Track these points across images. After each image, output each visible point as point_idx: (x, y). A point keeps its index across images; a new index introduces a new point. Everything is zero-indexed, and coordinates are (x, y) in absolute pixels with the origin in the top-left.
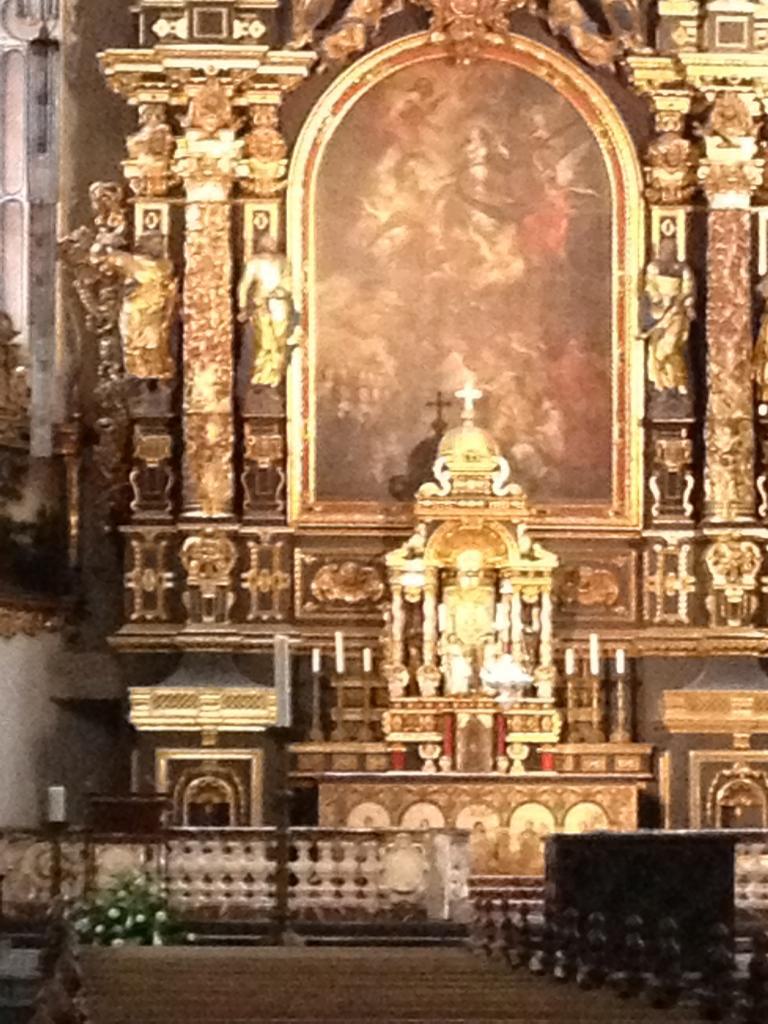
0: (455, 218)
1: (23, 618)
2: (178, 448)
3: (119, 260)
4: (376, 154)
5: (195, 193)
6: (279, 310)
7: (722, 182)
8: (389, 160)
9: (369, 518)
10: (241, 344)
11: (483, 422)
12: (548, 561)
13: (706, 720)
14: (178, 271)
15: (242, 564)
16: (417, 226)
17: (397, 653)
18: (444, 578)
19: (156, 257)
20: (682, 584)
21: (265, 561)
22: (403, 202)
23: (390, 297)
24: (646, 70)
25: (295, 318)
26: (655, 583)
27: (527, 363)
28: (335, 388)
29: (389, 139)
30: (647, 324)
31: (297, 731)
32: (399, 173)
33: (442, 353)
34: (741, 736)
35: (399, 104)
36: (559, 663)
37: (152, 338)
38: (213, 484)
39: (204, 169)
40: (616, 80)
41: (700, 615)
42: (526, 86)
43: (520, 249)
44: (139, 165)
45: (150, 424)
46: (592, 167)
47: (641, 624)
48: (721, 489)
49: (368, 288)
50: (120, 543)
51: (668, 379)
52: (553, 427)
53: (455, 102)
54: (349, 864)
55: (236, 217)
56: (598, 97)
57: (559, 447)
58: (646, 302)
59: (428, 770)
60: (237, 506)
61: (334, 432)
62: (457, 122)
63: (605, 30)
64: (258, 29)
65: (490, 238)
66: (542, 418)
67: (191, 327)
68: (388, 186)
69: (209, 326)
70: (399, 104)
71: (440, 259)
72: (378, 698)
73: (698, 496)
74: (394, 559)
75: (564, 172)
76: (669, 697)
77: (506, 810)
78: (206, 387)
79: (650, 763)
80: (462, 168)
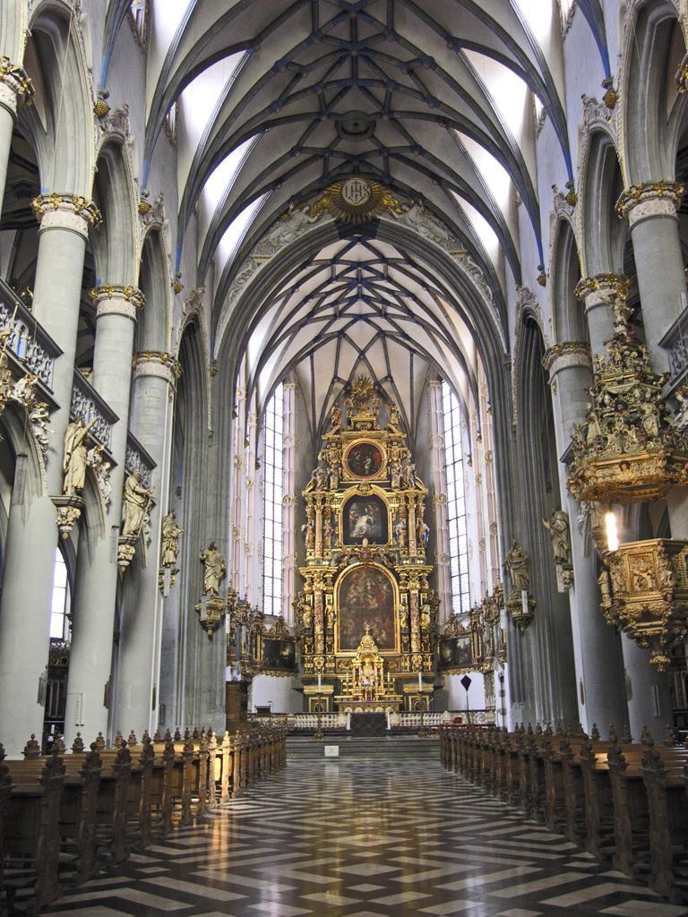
1: (286, 673)
2: (314, 640)
3: (303, 606)
4: (351, 585)
5: (316, 593)
6: (332, 614)
7: (412, 589)
8: (353, 586)
9: (352, 654)
10: (325, 620)
12: (382, 660)
13: (412, 690)
14: (313, 607)
15: (325, 662)
16: (358, 598)
17: (354, 679)
18: (363, 663)
19: (309, 605)
20: (408, 664)
21: (330, 662)
22: (355, 594)
23: (353, 612)
24: (398, 569)
25: (335, 616)
26: (403, 664)
28: (343, 628)
29: (353, 582)
30: (400, 615)
31: (333, 694)
32: (355, 589)
33: (363, 622)
35: (354, 576)
36: (386, 680)
37: (308, 620)
38: (320, 647)
39: (318, 590)
40: (393, 570)
41: (411, 670)
42: (377, 572)
43: (378, 602)
44: (307, 588)
45: (309, 636)
46: (390, 587)
47: (401, 672)
48: (414, 646)
49: (350, 610)
50: (303, 658)
51: (404, 626)
52: (384, 635)
53: (364, 575)
54: (331, 719)
55: (324, 598)
56: (391, 574)
57: (385, 639)
58: (400, 612)
59: (360, 701)
60: (324, 651)
62: (364, 579)
64: (328, 563)
65: (372, 600)
66: (382, 633)
68: (353, 591)
69: (319, 618)
70: (354, 576)
71: (362, 604)
74: (353, 661)
75: (385, 587)
76: (405, 685)
77: (374, 708)
78: (318, 629)
80: (366, 587)
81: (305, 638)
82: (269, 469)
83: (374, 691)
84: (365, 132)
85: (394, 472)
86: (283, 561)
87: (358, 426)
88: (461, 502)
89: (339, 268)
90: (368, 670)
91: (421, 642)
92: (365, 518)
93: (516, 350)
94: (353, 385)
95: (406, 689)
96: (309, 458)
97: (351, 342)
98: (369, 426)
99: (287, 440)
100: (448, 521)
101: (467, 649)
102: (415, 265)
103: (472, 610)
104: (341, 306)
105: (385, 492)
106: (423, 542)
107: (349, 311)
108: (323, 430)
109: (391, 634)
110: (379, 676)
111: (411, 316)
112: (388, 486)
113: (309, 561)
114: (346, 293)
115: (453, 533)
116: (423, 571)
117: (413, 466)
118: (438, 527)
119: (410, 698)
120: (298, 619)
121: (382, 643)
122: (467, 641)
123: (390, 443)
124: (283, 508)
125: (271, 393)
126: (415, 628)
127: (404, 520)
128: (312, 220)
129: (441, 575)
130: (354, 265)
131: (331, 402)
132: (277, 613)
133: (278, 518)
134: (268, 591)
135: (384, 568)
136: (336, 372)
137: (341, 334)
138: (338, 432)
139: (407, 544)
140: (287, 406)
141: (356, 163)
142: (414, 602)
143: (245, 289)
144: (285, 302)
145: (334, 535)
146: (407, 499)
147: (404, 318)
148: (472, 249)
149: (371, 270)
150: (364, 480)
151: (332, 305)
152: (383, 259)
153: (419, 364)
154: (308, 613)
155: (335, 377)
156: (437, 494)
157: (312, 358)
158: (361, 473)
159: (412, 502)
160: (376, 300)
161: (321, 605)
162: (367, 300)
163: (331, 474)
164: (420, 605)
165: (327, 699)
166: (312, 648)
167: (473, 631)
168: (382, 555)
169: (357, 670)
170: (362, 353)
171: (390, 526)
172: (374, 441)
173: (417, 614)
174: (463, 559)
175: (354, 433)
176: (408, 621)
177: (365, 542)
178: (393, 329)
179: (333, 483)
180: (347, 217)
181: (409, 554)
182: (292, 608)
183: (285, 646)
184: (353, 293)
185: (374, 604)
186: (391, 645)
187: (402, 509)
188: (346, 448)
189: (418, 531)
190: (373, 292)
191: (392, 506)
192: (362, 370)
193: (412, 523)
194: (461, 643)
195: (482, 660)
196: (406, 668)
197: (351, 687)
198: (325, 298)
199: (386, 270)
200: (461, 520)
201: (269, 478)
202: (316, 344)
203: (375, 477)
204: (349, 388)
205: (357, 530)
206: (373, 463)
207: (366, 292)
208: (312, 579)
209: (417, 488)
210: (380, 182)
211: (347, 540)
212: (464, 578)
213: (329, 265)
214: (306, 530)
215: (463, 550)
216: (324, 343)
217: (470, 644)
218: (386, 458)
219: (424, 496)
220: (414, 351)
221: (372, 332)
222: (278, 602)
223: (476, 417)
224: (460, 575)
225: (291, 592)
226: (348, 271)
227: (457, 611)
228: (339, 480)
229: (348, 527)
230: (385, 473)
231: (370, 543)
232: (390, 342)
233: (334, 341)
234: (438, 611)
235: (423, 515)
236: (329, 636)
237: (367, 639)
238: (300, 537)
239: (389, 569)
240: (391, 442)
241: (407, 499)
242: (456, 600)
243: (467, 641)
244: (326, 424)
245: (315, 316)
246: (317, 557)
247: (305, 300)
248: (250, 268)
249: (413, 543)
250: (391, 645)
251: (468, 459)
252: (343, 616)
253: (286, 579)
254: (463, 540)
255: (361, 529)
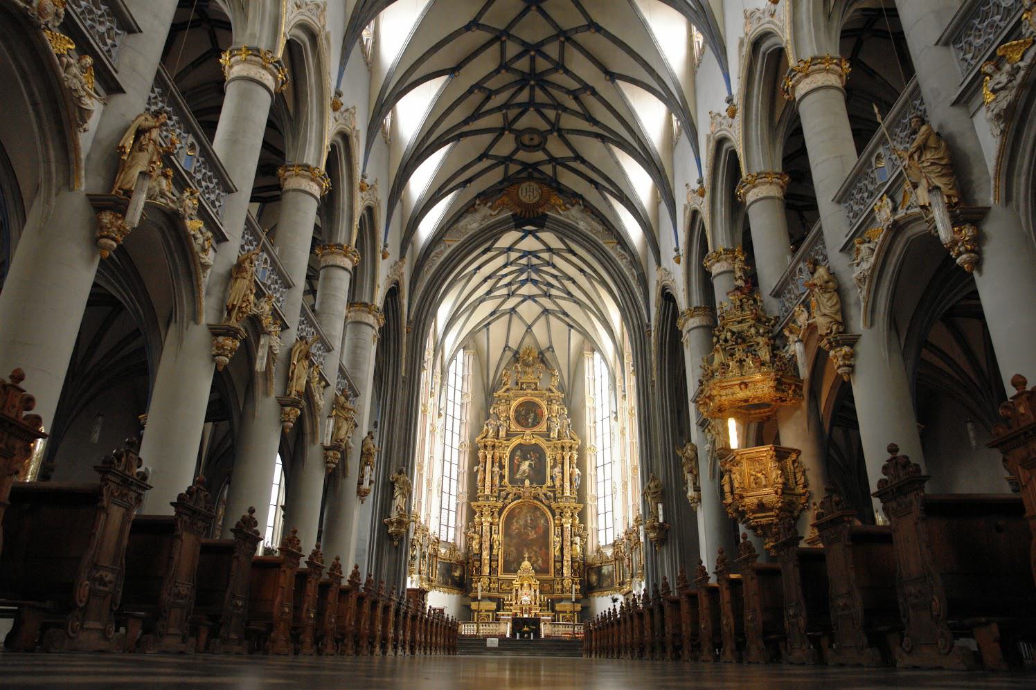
0: (525, 528)
1: (456, 591)
6: (497, 543)
8: (515, 519)
11: (529, 560)
12: (538, 583)
13: (563, 609)
15: (490, 583)
18: (522, 585)
20: (560, 587)
21: (494, 582)
24: (554, 505)
27: (536, 552)
28: (506, 554)
32: (517, 522)
34: (568, 612)
37: (477, 547)
38: (486, 570)
40: (549, 507)
41: (562, 592)
43: (536, 533)
44: (477, 519)
45: (477, 560)
46: (547, 521)
51: (557, 554)
52: (540, 562)
53: (525, 511)
56: (547, 510)
61: (506, 562)
63: (548, 499)
67: (483, 545)
69: (486, 545)
72: (511, 605)
73: (562, 573)
74: (514, 582)
75: (542, 521)
78: (485, 554)
79: (554, 616)
80: (526, 521)
81: (473, 562)
82: (449, 419)
83: (530, 609)
84: (538, 145)
85: (553, 425)
86: (457, 496)
87: (524, 386)
88: (607, 452)
89: (514, 255)
90: (526, 590)
91: (572, 568)
92: (527, 463)
93: (655, 327)
94: (521, 352)
95: (558, 608)
96: (483, 414)
97: (521, 318)
98: (533, 386)
99: (465, 396)
100: (596, 467)
101: (610, 575)
102: (575, 254)
103: (615, 541)
104: (513, 287)
105: (546, 442)
106: (575, 484)
107: (520, 292)
108: (494, 390)
109: (546, 561)
110: (535, 596)
111: (569, 293)
112: (547, 436)
113: (479, 497)
114: (518, 276)
115: (600, 478)
116: (575, 508)
117: (569, 420)
118: (588, 472)
119: (561, 615)
120: (468, 546)
121: (538, 568)
122: (610, 568)
123: (550, 401)
124: (459, 452)
125: (454, 357)
126: (567, 557)
127: (560, 465)
128: (493, 213)
129: (590, 513)
130: (526, 254)
131: (502, 366)
132: (450, 540)
133: (455, 460)
134: (444, 521)
135: (542, 505)
136: (507, 341)
137: (513, 310)
138: (508, 390)
139: (562, 486)
140: (466, 369)
141: (530, 170)
142: (567, 534)
143: (436, 266)
144: (468, 281)
145: (502, 477)
146: (563, 448)
147: (564, 299)
148: (621, 240)
149: (539, 258)
150: (528, 432)
151: (506, 285)
152: (549, 250)
153: (575, 337)
154: (478, 541)
155: (507, 346)
156: (588, 445)
157: (488, 329)
158: (526, 426)
159: (567, 450)
160: (542, 283)
161: (489, 534)
162: (535, 282)
163: (500, 425)
164: (571, 537)
165: (491, 614)
166: (479, 571)
167: (616, 559)
168: (541, 494)
169: (517, 590)
170: (529, 327)
171: (548, 469)
172: (537, 399)
173: (569, 544)
174: (609, 499)
175: (521, 392)
176: (562, 549)
177: (527, 482)
178: (556, 309)
179: (502, 433)
180: (522, 212)
181: (563, 494)
182: (463, 536)
183: (456, 568)
184: (524, 277)
185: (532, 535)
186: (547, 571)
187: (559, 456)
188: (514, 404)
189: (571, 475)
190: (540, 276)
191: (548, 453)
192: (528, 341)
193: (567, 467)
194: (605, 570)
195: (621, 584)
196: (558, 590)
197: (511, 605)
198: (501, 279)
199: (551, 258)
200: (608, 467)
201: (449, 427)
202: (492, 318)
203: (537, 429)
204: (517, 356)
205: (520, 472)
206: (536, 416)
207: (534, 276)
208: (481, 512)
209: (572, 438)
210: (549, 185)
211: (512, 481)
212: (609, 515)
213: (505, 252)
214: (477, 471)
215: (608, 491)
216: (498, 318)
217: (613, 571)
218: (546, 413)
219: (577, 446)
220: (572, 327)
221: (540, 310)
222: (452, 531)
223: (622, 381)
224: (605, 513)
225: (463, 522)
226: (521, 258)
227: (602, 543)
228: (507, 431)
229: (514, 469)
230: (546, 426)
231: (531, 483)
232: (552, 318)
233: (506, 317)
234: (586, 544)
235: (575, 461)
236: (494, 560)
237: (526, 564)
238: (472, 476)
239: (546, 506)
240: (551, 401)
241: (563, 448)
242: (602, 534)
243: (610, 568)
244: (498, 384)
245: (492, 295)
246: (486, 493)
247: (485, 280)
248: (443, 247)
249: (567, 484)
250: (547, 571)
251: (614, 415)
252: (507, 545)
253: (460, 513)
254: (608, 483)
255: (524, 472)
